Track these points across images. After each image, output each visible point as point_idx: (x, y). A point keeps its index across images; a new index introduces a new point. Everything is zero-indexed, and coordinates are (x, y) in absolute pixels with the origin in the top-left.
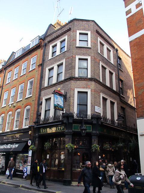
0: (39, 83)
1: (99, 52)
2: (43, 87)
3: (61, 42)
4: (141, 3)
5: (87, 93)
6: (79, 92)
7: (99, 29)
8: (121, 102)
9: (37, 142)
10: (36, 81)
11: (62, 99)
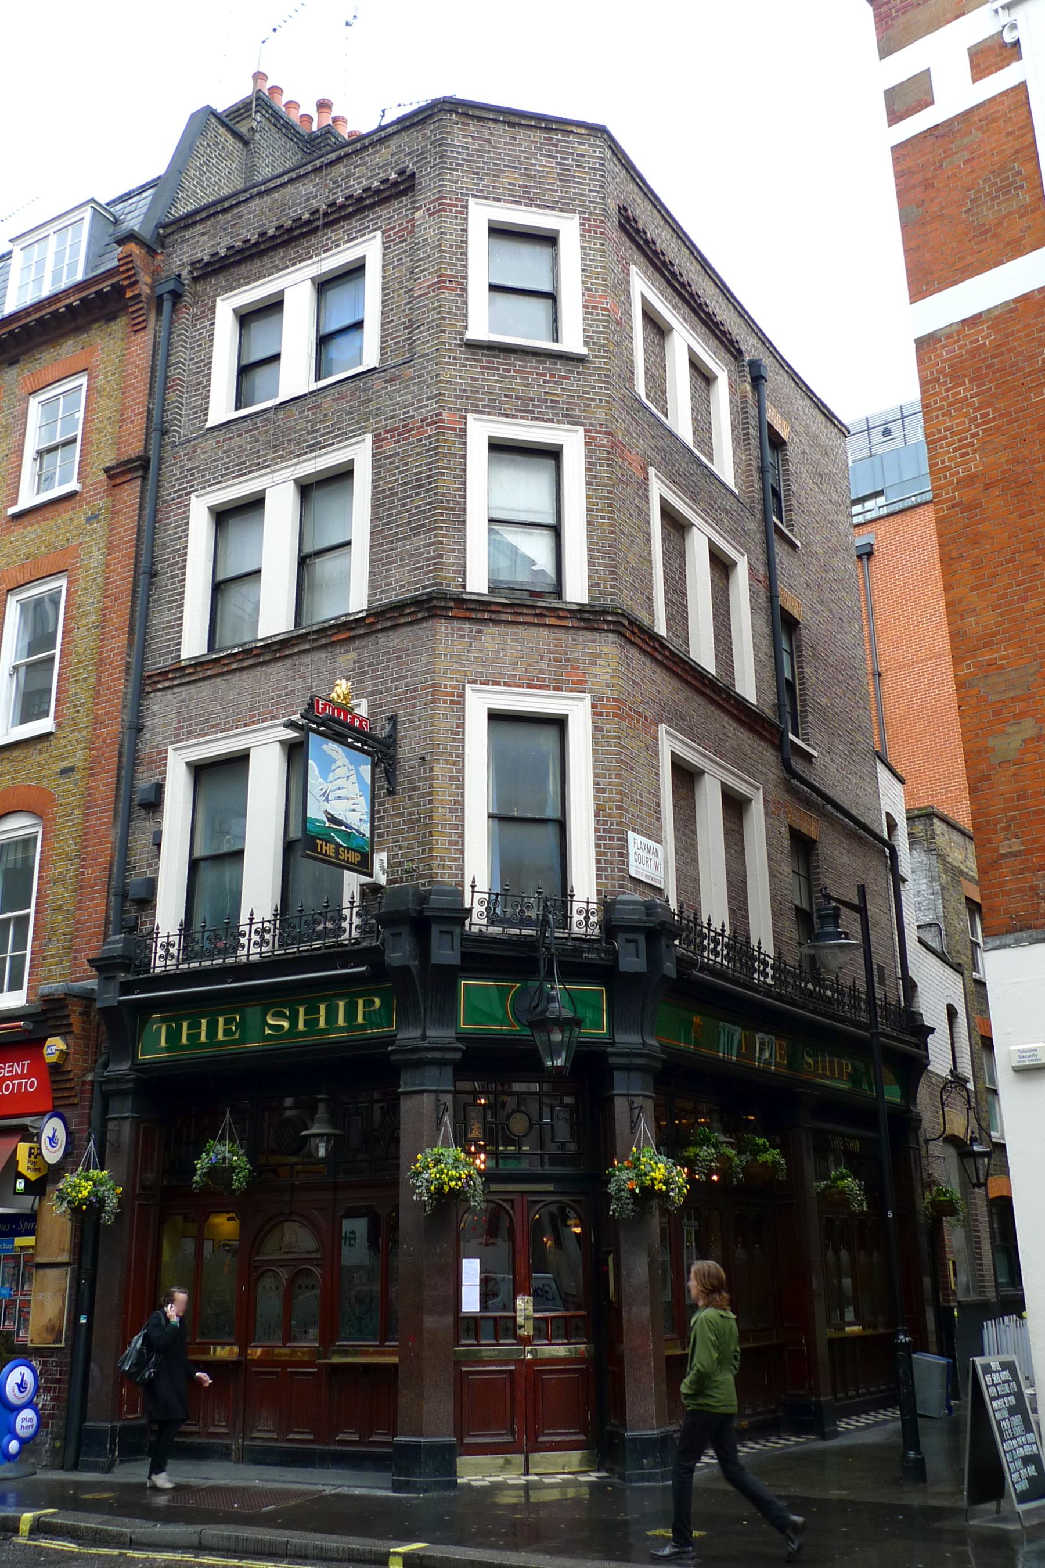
0: (119, 618)
1: (640, 388)
2: (158, 663)
3: (324, 286)
4: (1017, 43)
5: (559, 723)
6: (496, 717)
7: (639, 197)
8: (791, 790)
9: (123, 1132)
10: (90, 601)
11: (366, 770)
